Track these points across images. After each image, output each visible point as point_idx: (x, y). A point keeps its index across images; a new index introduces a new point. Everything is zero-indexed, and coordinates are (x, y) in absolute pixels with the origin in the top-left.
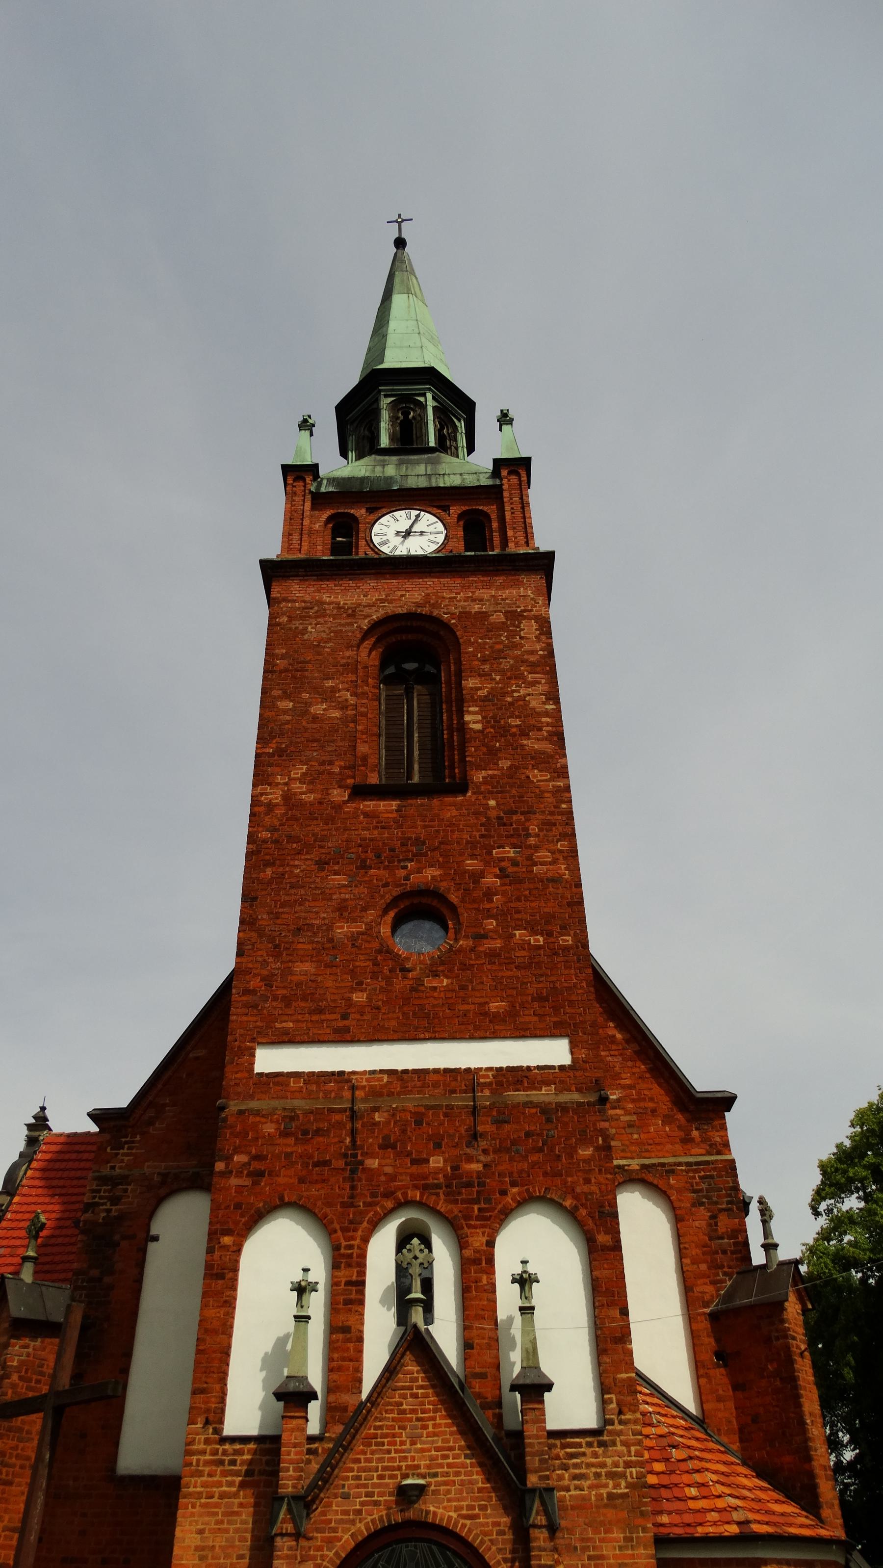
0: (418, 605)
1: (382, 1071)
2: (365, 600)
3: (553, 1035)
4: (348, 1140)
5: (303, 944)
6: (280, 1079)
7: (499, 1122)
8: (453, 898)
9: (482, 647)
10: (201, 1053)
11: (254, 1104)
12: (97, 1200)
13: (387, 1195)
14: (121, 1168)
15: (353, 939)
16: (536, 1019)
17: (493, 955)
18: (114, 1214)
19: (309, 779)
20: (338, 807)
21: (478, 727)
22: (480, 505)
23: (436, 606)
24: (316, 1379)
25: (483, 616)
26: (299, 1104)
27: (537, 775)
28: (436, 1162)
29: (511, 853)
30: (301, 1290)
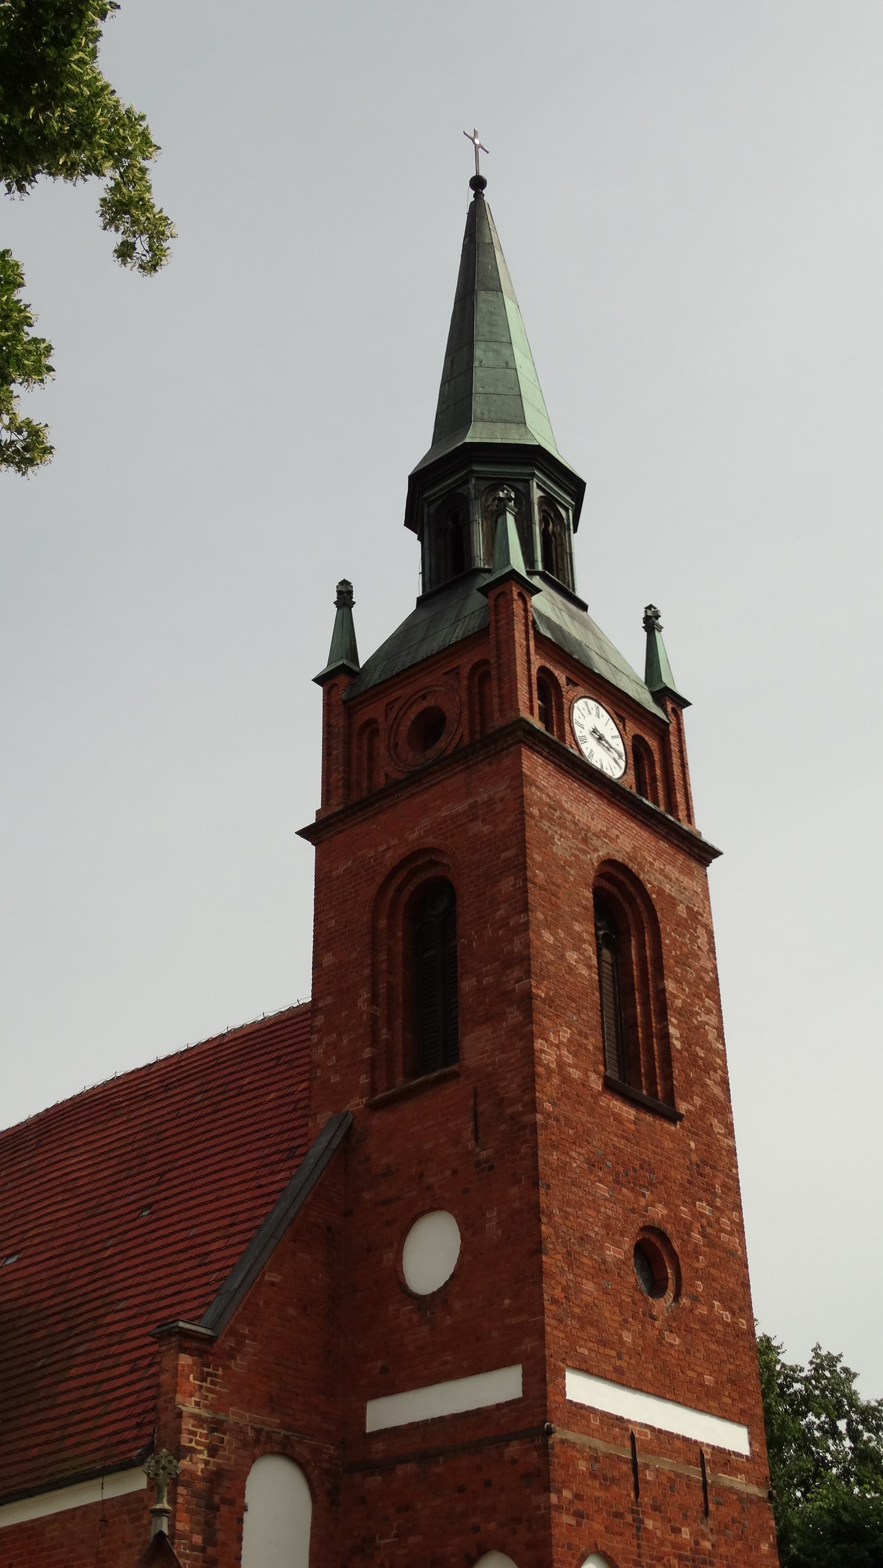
1: (647, 1426)
3: (740, 1423)
4: (633, 1495)
6: (583, 1412)
8: (676, 1245)
12: (193, 1445)
14: (205, 1407)
16: (729, 1401)
17: (706, 1323)
18: (210, 1467)
22: (647, 734)
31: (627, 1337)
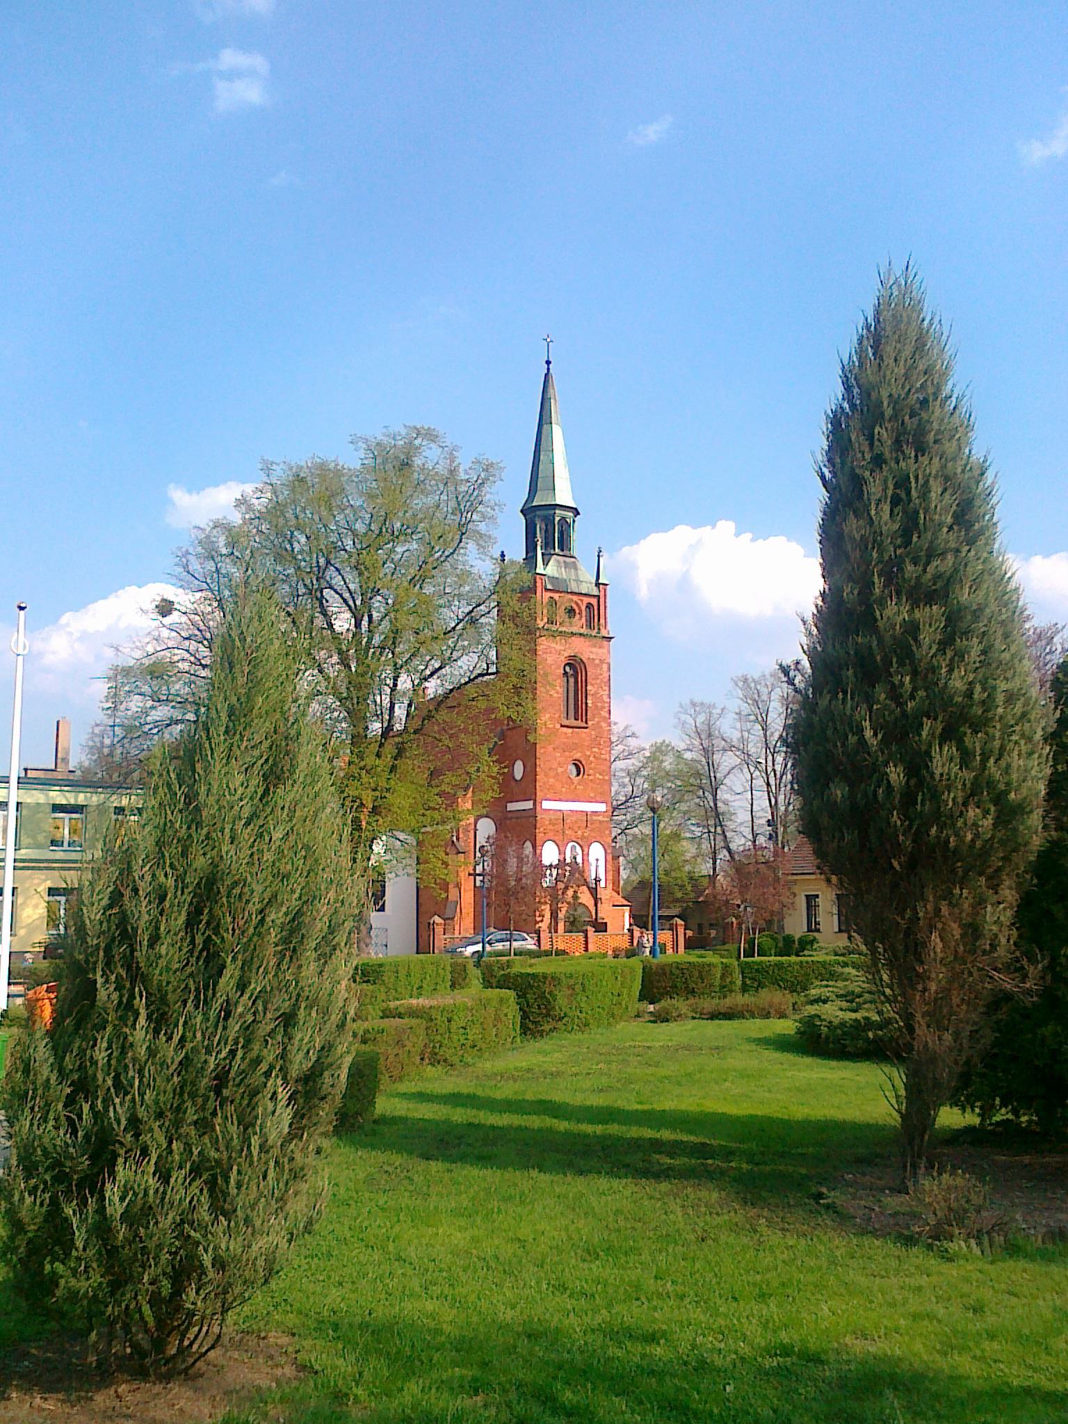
5: (552, 773)
19: (551, 719)
27: (604, 724)
29: (595, 750)
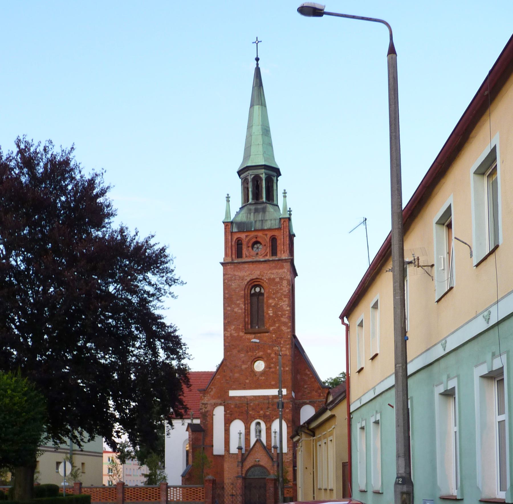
0: (259, 276)
2: (246, 274)
7: (273, 405)
9: (273, 290)
10: (219, 377)
11: (230, 402)
13: (253, 418)
15: (246, 368)
17: (273, 372)
19: (235, 330)
20: (242, 337)
21: (271, 314)
23: (263, 276)
24: (243, 446)
25: (274, 279)
26: (238, 402)
28: (261, 412)
29: (277, 348)
30: (240, 434)
31: (247, 381)
